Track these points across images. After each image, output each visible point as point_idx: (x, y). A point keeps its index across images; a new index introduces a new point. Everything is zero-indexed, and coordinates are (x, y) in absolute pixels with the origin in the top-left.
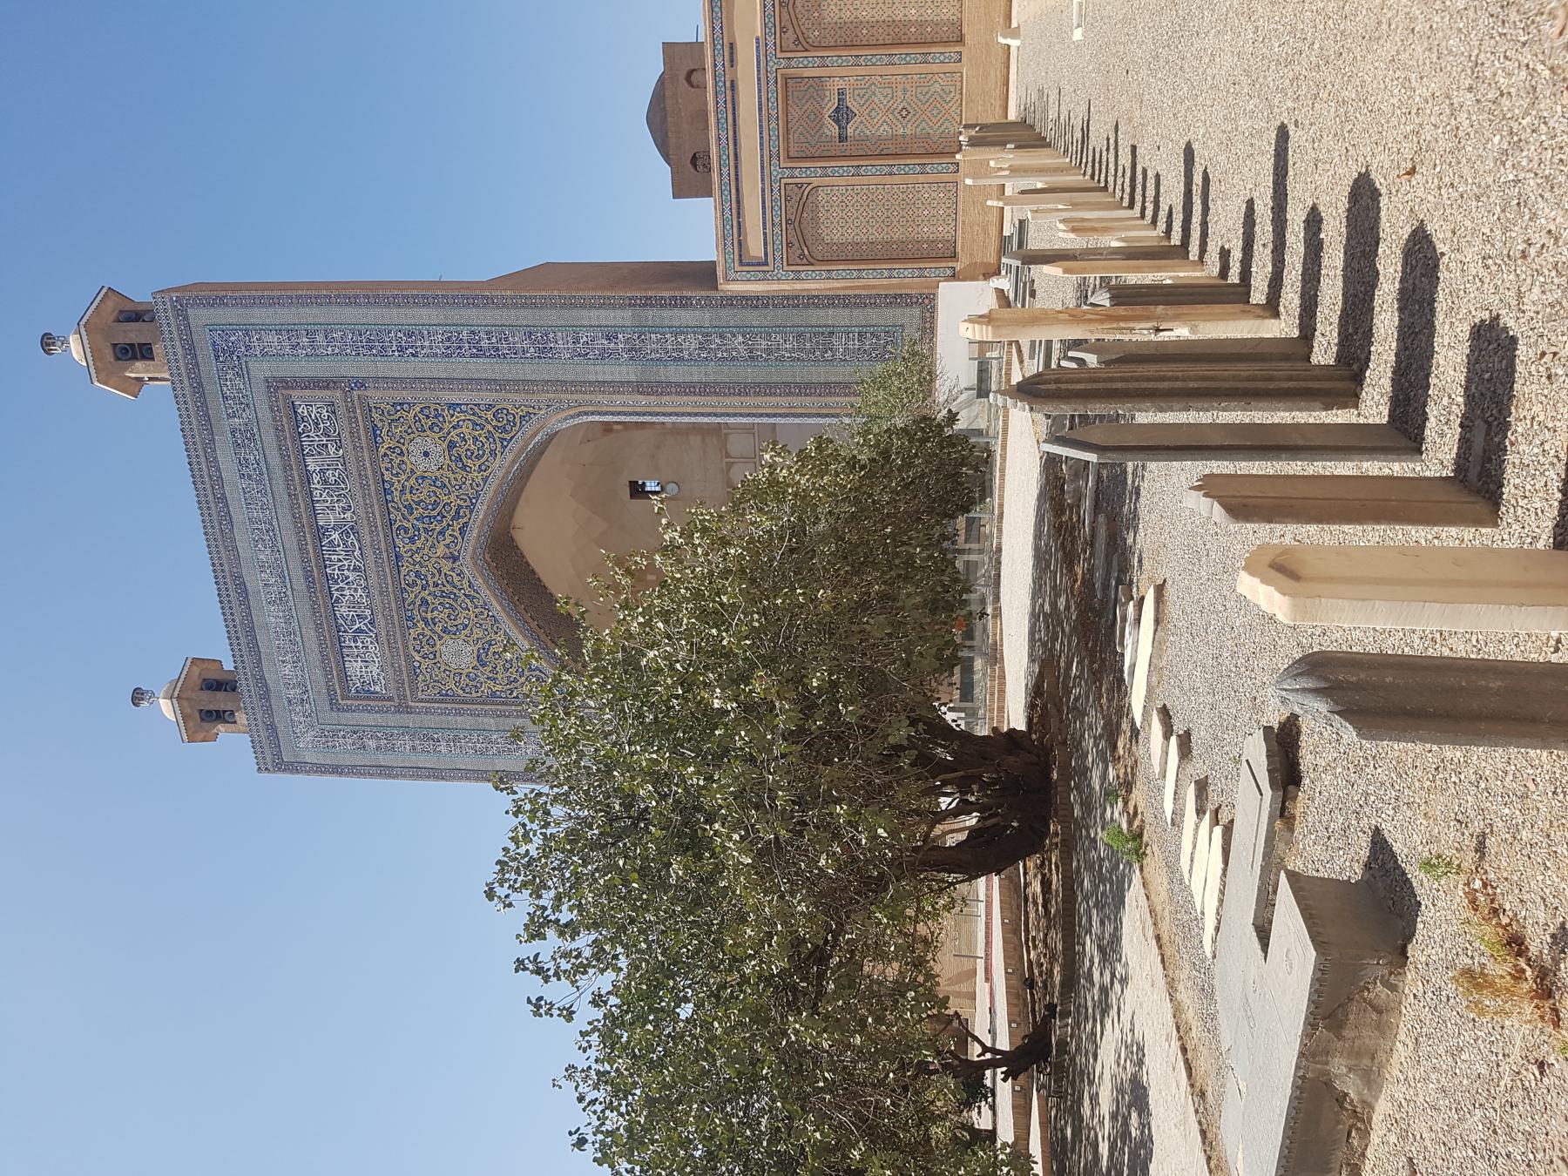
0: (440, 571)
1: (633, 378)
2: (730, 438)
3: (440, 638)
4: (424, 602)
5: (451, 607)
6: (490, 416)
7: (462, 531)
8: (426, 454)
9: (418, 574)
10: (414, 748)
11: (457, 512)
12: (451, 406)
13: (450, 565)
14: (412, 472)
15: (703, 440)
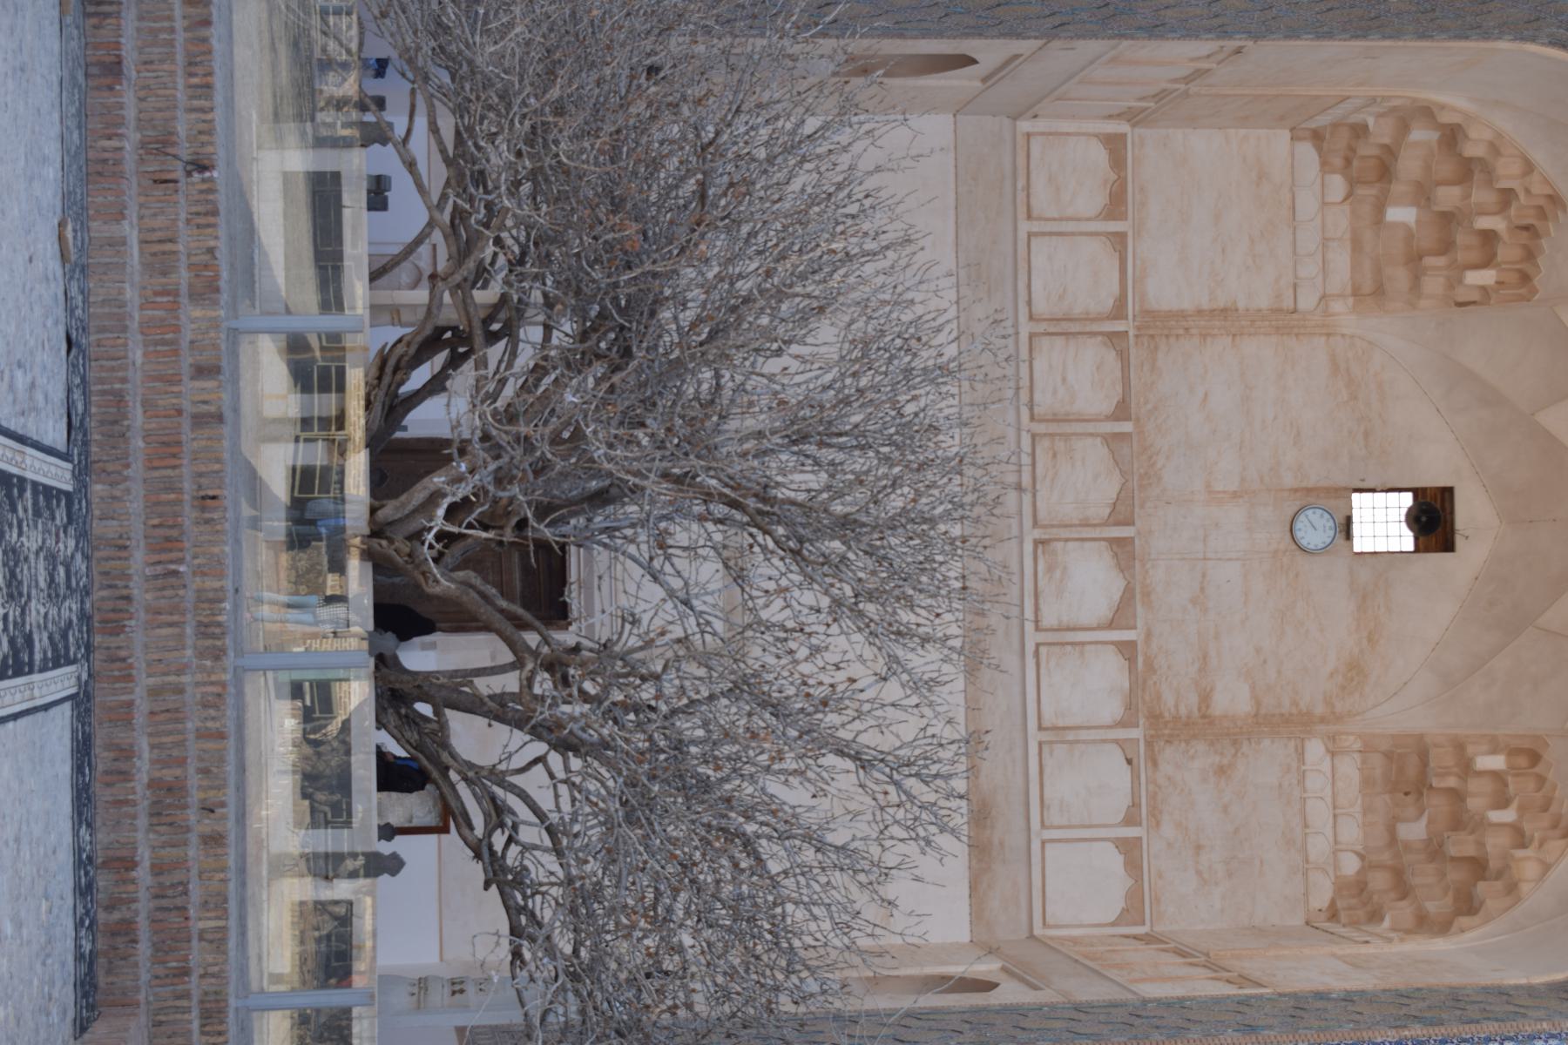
2: (1112, 709)
15: (1205, 698)
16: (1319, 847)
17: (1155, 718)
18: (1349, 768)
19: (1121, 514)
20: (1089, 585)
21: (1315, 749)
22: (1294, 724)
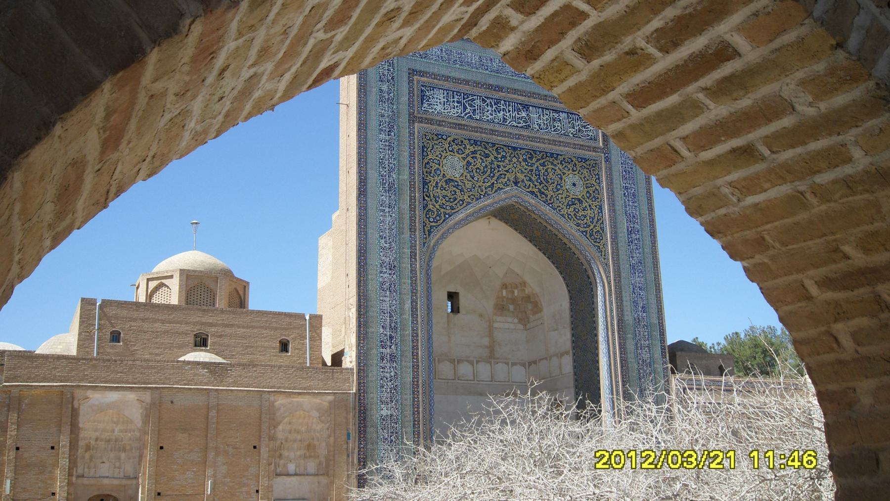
0: (507, 171)
1: (626, 318)
3: (464, 159)
4: (487, 156)
5: (484, 172)
6: (598, 228)
7: (532, 193)
8: (574, 185)
9: (503, 157)
10: (383, 116)
11: (543, 193)
12: (601, 208)
13: (512, 179)
14: (564, 174)
15: (486, 347)
16: (512, 326)
17: (490, 357)
18: (499, 319)
19: (452, 361)
20: (465, 369)
21: (495, 325)
22: (491, 331)
